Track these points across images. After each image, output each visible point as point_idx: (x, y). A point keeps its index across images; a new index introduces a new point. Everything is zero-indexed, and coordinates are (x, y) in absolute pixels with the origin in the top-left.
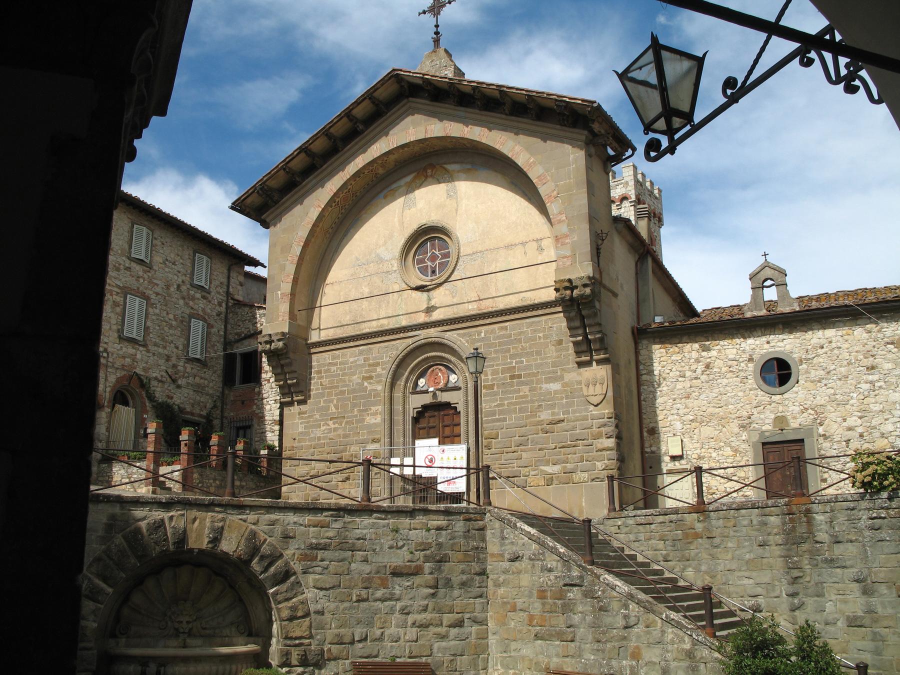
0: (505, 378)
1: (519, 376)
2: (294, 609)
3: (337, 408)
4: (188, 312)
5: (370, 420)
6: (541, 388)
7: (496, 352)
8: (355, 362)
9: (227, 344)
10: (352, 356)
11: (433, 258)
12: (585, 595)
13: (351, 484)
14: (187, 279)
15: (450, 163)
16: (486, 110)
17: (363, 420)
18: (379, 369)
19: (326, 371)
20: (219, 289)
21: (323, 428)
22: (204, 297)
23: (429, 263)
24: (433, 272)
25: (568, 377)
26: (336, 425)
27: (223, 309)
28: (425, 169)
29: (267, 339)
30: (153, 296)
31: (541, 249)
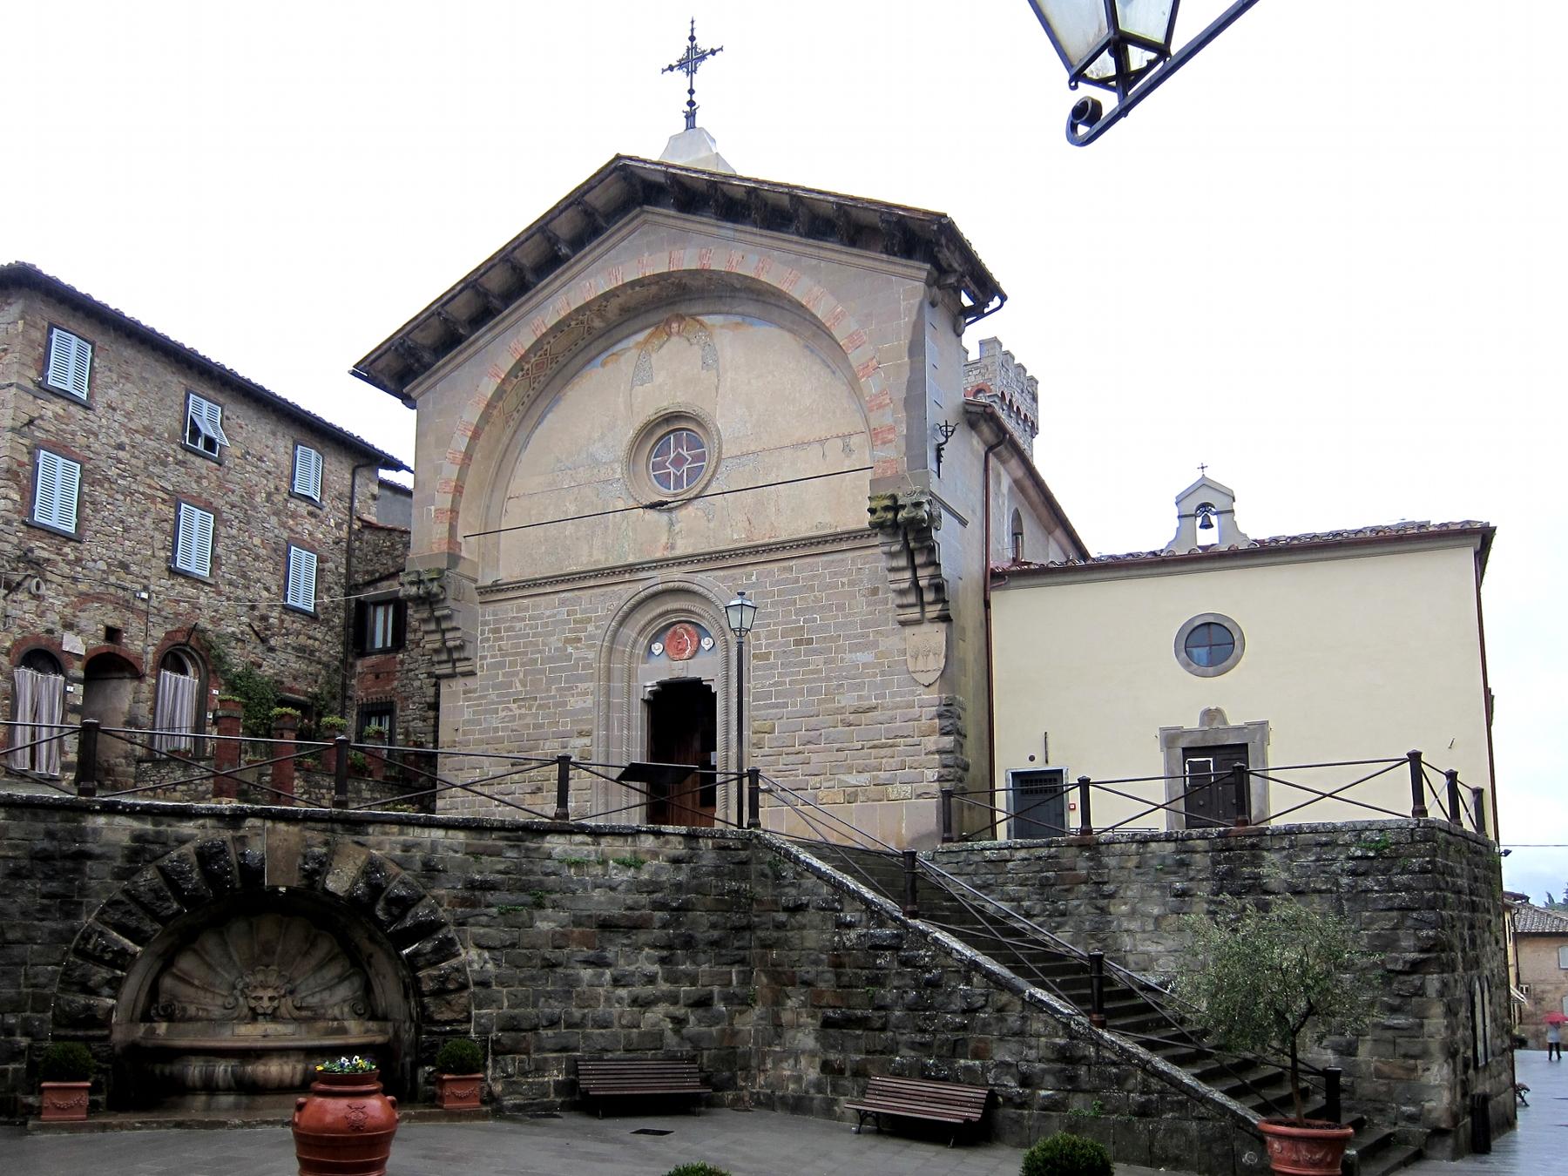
0: (787, 644)
2: (444, 979)
4: (285, 535)
5: (575, 703)
6: (842, 660)
7: (773, 604)
9: (351, 588)
10: (549, 607)
11: (678, 461)
12: (905, 963)
14: (284, 485)
16: (768, 228)
17: (565, 704)
18: (590, 628)
19: (507, 630)
20: (336, 503)
22: (311, 514)
23: (672, 470)
24: (679, 483)
25: (884, 644)
27: (344, 534)
28: (668, 322)
29: (413, 578)
30: (226, 508)
31: (847, 450)
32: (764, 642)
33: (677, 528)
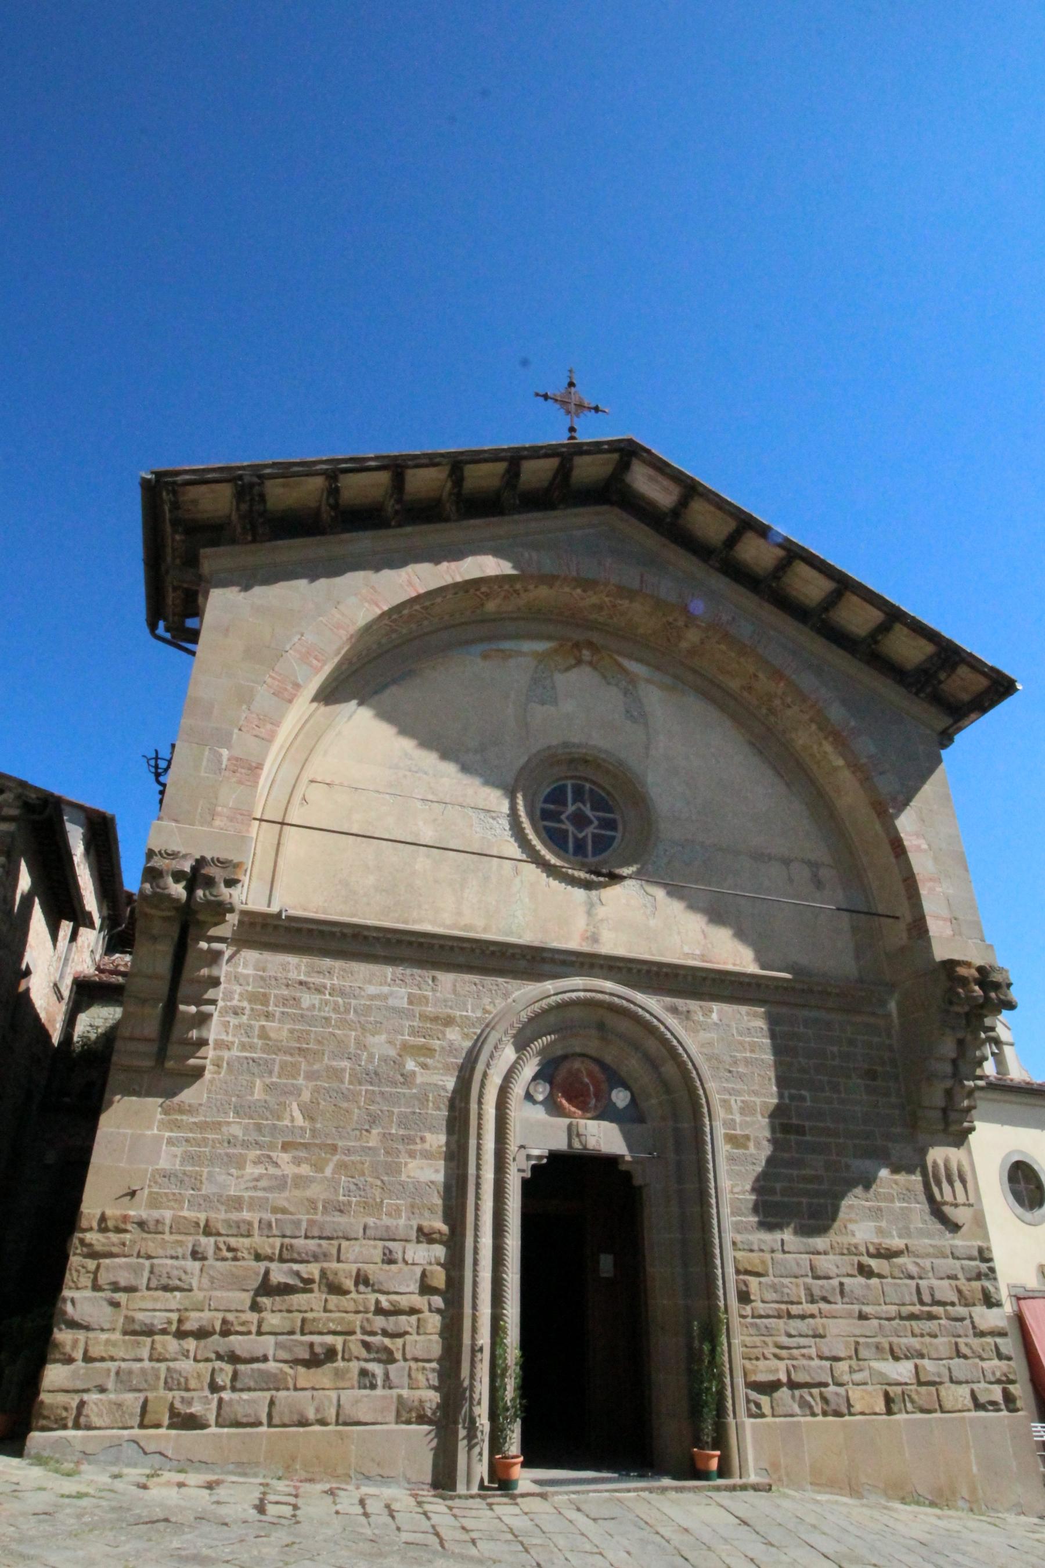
1: (800, 1130)
3: (309, 1115)
6: (848, 1167)
8: (385, 997)
11: (579, 820)
13: (338, 1374)
15: (630, 657)
19: (285, 1001)
21: (252, 1170)
26: (305, 1170)
32: (738, 1118)
33: (601, 912)
